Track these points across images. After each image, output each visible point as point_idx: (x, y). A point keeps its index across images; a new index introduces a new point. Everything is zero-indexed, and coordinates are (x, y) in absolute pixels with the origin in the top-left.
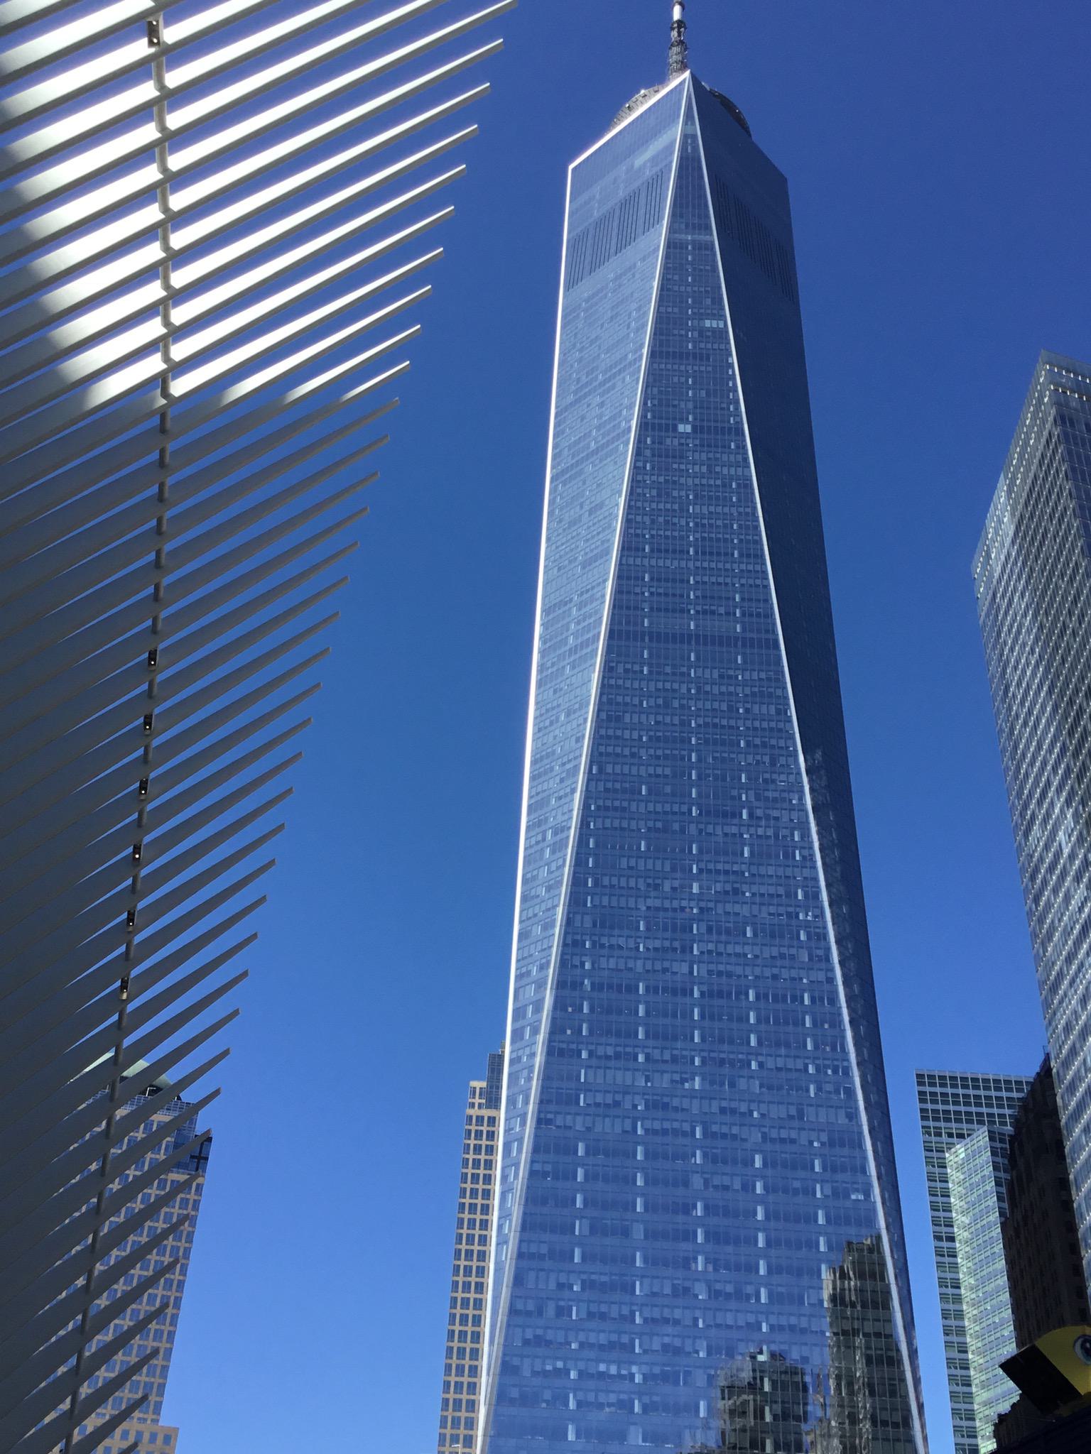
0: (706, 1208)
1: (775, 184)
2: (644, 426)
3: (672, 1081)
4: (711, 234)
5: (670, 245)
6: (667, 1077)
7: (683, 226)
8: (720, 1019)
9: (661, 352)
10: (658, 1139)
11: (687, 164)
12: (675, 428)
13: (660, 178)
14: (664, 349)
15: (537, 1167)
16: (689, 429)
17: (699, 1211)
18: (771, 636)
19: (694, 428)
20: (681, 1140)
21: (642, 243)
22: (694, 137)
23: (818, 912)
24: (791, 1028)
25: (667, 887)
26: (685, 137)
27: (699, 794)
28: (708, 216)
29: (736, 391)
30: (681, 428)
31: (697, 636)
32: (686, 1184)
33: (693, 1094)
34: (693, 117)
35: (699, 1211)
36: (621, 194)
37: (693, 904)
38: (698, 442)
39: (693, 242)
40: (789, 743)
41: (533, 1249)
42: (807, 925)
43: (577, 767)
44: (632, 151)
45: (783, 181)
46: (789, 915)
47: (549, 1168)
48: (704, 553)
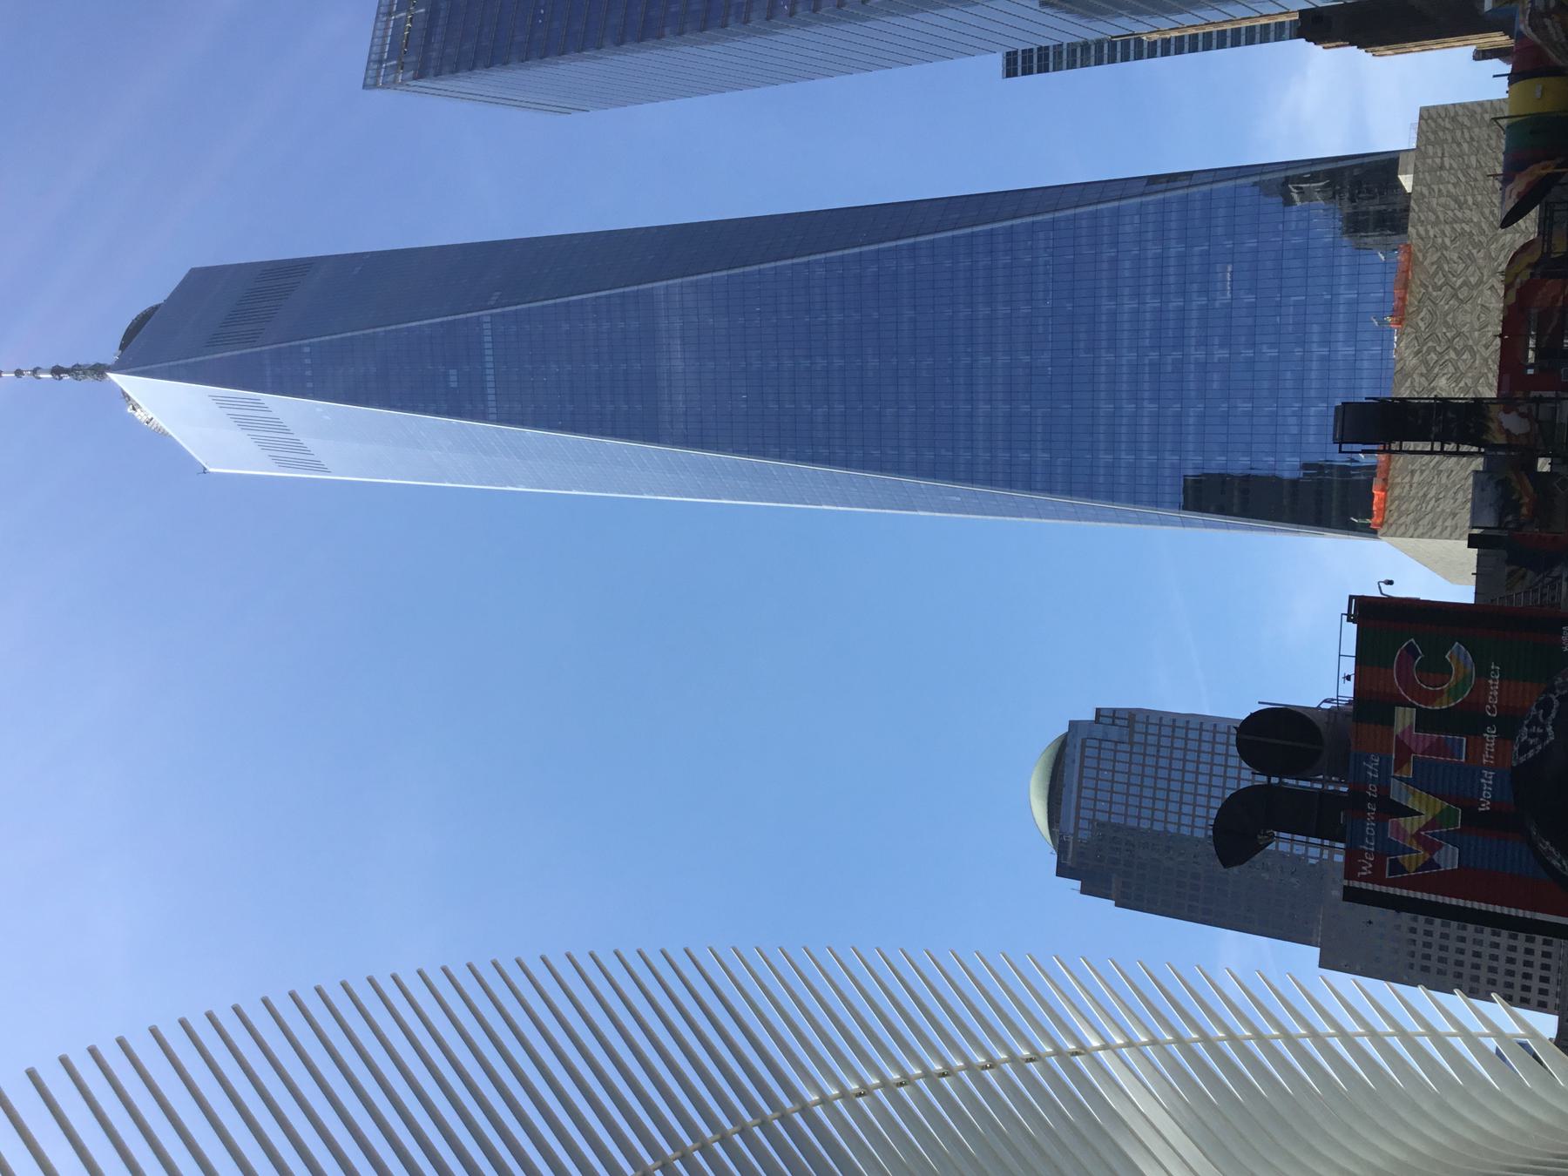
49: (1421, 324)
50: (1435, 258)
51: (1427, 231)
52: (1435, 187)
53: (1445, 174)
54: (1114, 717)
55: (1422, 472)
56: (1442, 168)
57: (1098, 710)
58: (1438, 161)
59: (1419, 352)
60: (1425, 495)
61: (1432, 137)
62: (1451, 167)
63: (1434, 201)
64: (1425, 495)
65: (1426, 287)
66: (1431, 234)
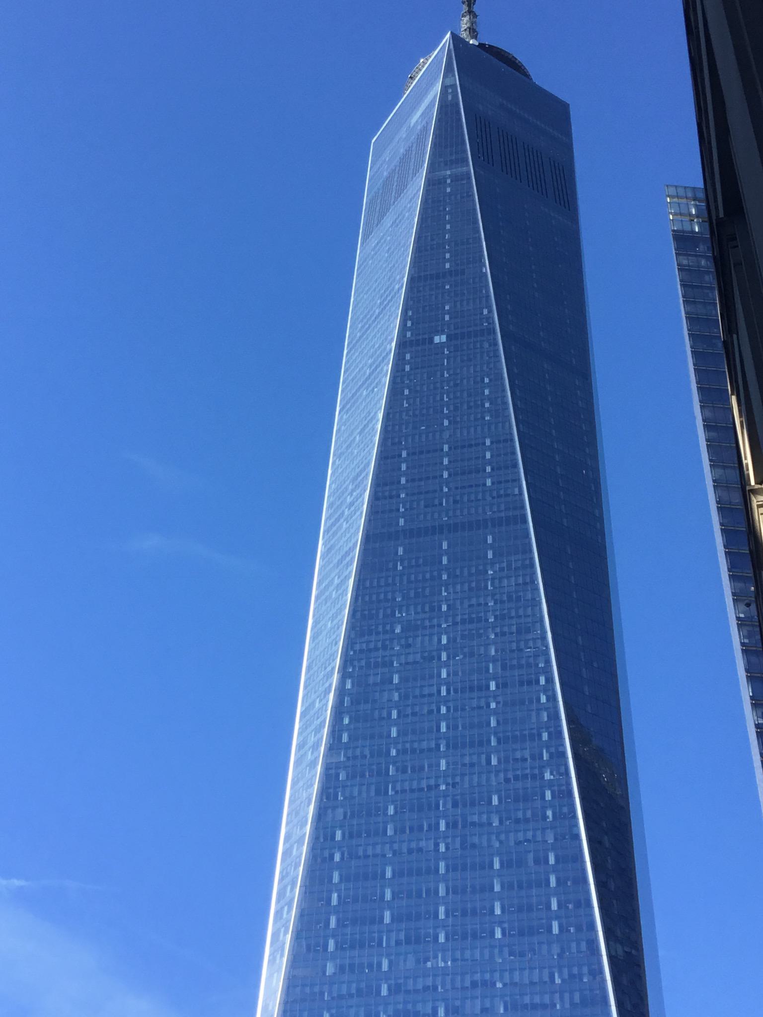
1: (557, 113)
4: (468, 165)
5: (432, 184)
7: (442, 164)
9: (420, 277)
11: (446, 109)
12: (431, 340)
13: (425, 129)
14: (422, 274)
16: (444, 338)
18: (517, 513)
21: (410, 191)
26: (445, 88)
30: (437, 339)
34: (453, 70)
36: (402, 151)
38: (452, 349)
44: (410, 114)
45: (565, 107)
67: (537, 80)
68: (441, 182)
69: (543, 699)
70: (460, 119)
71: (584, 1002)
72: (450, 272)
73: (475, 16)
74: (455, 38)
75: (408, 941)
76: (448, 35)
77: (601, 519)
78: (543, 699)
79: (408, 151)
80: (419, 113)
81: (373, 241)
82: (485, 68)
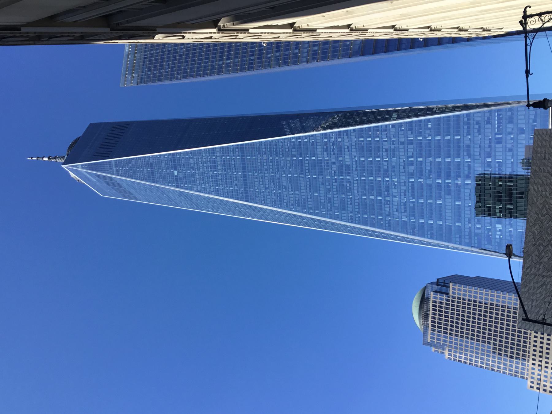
0: (438, 179)
1: (93, 128)
2: (178, 186)
3: (395, 188)
6: (394, 190)
8: (372, 170)
10: (416, 194)
11: (90, 167)
12: (176, 176)
15: (429, 236)
16: (175, 172)
17: (440, 181)
19: (175, 170)
20: (415, 185)
22: (82, 165)
23: (331, 135)
24: (373, 146)
25: (329, 187)
26: (82, 168)
27: (297, 174)
28: (106, 162)
29: (160, 155)
30: (176, 174)
31: (243, 172)
32: (430, 186)
33: (399, 182)
35: (440, 181)
37: (333, 178)
39: (116, 167)
40: (274, 142)
41: (458, 239)
42: (336, 138)
43: (293, 215)
44: (91, 181)
45: (91, 125)
46: (333, 144)
47: (429, 233)
48: (215, 168)
49: (536, 232)
50: (542, 202)
51: (538, 188)
52: (542, 168)
53: (546, 162)
54: (444, 283)
55: (537, 301)
56: (545, 159)
57: (438, 280)
58: (543, 155)
59: (535, 245)
60: (539, 312)
61: (540, 144)
62: (549, 159)
63: (541, 175)
64: (539, 312)
65: (538, 214)
66: (540, 189)
67: (80, 134)
68: (117, 171)
69: (306, 140)
70: (94, 163)
71: (411, 129)
72: (151, 168)
73: (56, 157)
74: (64, 164)
75: (388, 191)
76: (63, 166)
77: (243, 117)
78: (306, 140)
79: (106, 183)
80: (91, 178)
81: (138, 196)
82: (75, 153)
